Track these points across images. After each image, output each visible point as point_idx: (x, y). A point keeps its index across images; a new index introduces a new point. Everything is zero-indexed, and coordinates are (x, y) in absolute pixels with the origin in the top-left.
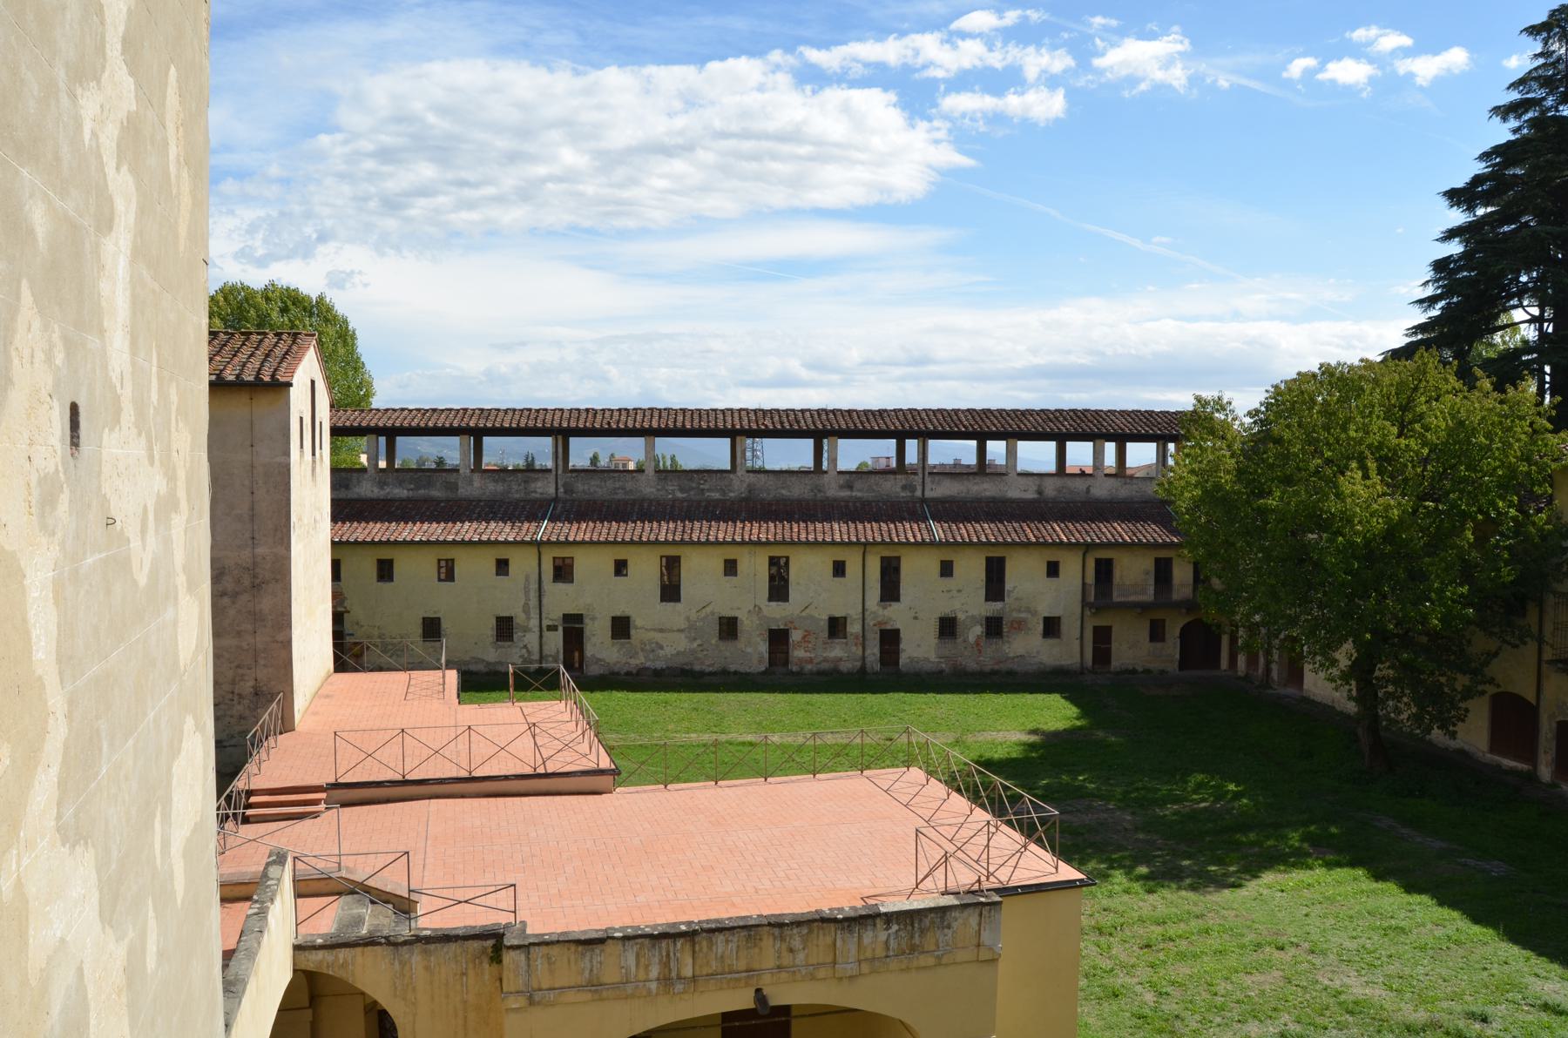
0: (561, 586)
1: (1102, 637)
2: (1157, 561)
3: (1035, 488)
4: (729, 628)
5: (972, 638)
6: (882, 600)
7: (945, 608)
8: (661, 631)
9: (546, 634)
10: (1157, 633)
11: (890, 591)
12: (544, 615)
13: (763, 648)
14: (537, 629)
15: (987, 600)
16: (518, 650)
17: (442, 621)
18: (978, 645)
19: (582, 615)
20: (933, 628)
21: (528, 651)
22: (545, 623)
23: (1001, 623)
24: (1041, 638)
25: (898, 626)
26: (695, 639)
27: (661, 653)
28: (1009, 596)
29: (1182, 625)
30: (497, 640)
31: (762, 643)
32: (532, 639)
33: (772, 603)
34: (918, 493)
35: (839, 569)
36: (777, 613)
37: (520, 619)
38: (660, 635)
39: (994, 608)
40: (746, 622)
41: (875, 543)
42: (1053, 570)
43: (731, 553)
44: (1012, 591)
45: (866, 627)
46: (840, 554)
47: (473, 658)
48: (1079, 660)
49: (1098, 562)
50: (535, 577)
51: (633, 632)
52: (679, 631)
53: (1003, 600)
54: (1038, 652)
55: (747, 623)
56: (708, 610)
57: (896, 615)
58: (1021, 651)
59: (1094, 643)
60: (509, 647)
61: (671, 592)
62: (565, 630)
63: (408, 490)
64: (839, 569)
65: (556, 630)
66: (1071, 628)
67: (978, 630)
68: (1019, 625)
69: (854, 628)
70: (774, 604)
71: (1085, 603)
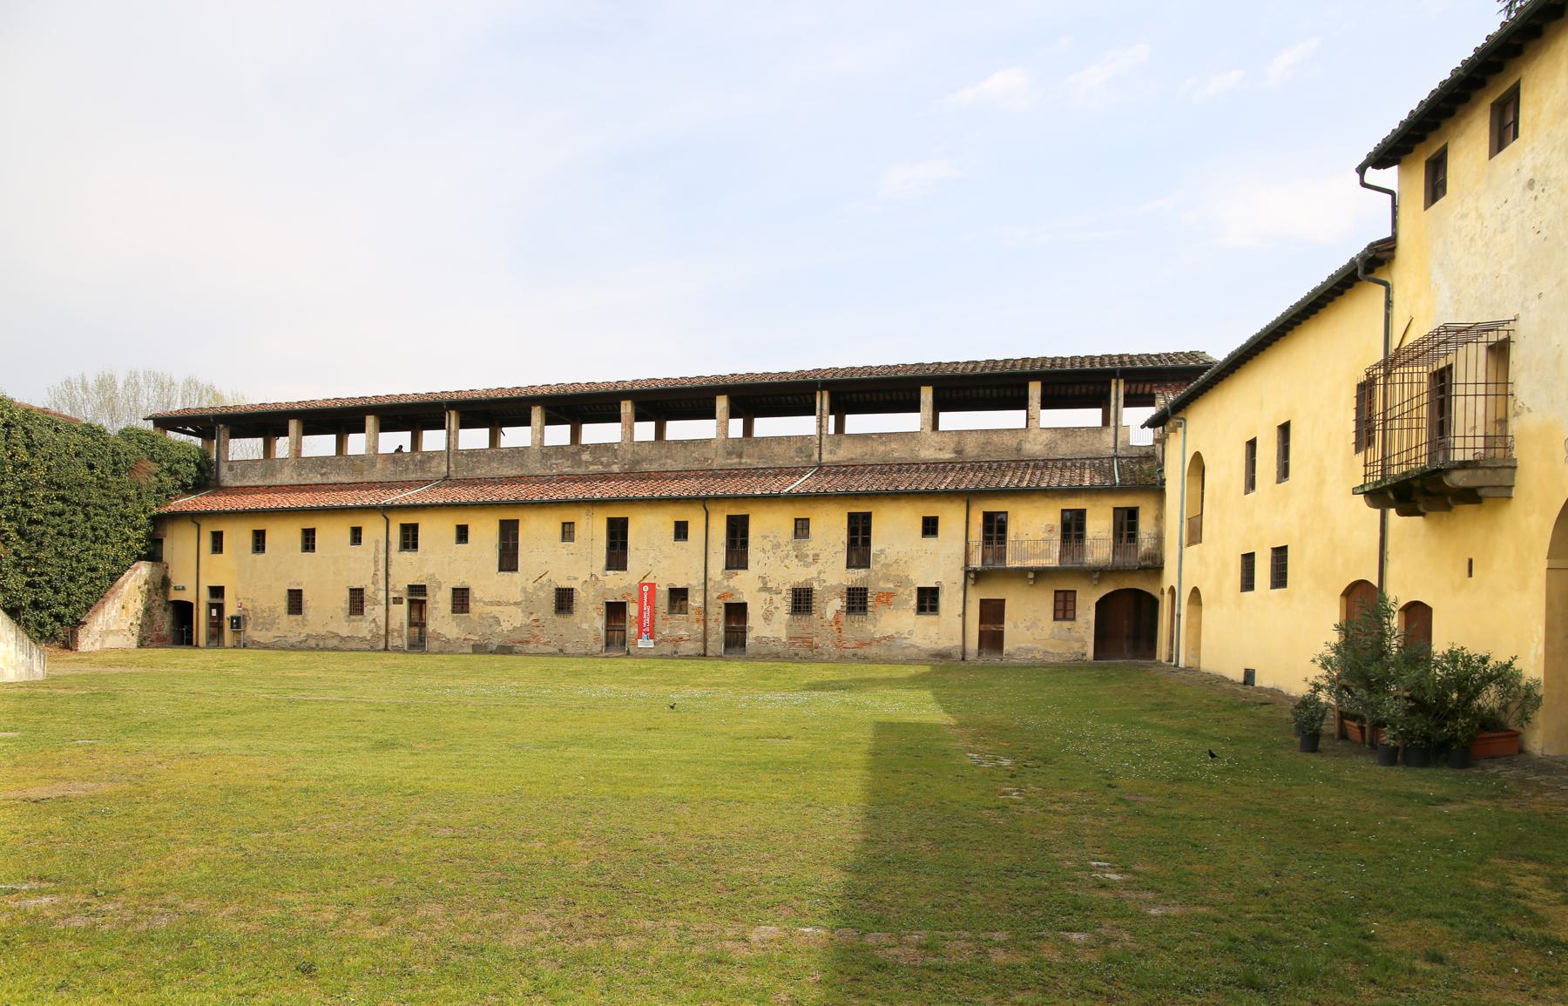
0: (407, 555)
1: (992, 612)
3: (952, 446)
4: (564, 600)
5: (830, 615)
6: (727, 568)
7: (799, 575)
8: (499, 604)
9: (393, 607)
10: (1064, 608)
12: (390, 587)
13: (600, 623)
14: (384, 602)
15: (848, 566)
16: (365, 624)
17: (304, 593)
18: (837, 623)
19: (425, 586)
20: (783, 605)
21: (377, 625)
22: (392, 595)
23: (866, 594)
25: (745, 599)
26: (532, 613)
27: (499, 630)
29: (1101, 596)
30: (351, 614)
31: (598, 618)
32: (380, 611)
33: (609, 572)
35: (681, 531)
36: (617, 584)
37: (368, 593)
38: (498, 608)
39: (856, 577)
40: (583, 594)
42: (930, 527)
45: (708, 598)
46: (682, 513)
47: (330, 632)
48: (959, 642)
51: (471, 605)
52: (516, 604)
54: (910, 633)
55: (581, 597)
56: (544, 579)
57: (744, 586)
58: (890, 631)
59: (981, 622)
60: (360, 620)
61: (508, 559)
62: (411, 602)
63: (322, 475)
64: (681, 531)
65: (402, 603)
66: (950, 602)
67: (837, 604)
68: (887, 598)
69: (695, 601)
70: (610, 573)
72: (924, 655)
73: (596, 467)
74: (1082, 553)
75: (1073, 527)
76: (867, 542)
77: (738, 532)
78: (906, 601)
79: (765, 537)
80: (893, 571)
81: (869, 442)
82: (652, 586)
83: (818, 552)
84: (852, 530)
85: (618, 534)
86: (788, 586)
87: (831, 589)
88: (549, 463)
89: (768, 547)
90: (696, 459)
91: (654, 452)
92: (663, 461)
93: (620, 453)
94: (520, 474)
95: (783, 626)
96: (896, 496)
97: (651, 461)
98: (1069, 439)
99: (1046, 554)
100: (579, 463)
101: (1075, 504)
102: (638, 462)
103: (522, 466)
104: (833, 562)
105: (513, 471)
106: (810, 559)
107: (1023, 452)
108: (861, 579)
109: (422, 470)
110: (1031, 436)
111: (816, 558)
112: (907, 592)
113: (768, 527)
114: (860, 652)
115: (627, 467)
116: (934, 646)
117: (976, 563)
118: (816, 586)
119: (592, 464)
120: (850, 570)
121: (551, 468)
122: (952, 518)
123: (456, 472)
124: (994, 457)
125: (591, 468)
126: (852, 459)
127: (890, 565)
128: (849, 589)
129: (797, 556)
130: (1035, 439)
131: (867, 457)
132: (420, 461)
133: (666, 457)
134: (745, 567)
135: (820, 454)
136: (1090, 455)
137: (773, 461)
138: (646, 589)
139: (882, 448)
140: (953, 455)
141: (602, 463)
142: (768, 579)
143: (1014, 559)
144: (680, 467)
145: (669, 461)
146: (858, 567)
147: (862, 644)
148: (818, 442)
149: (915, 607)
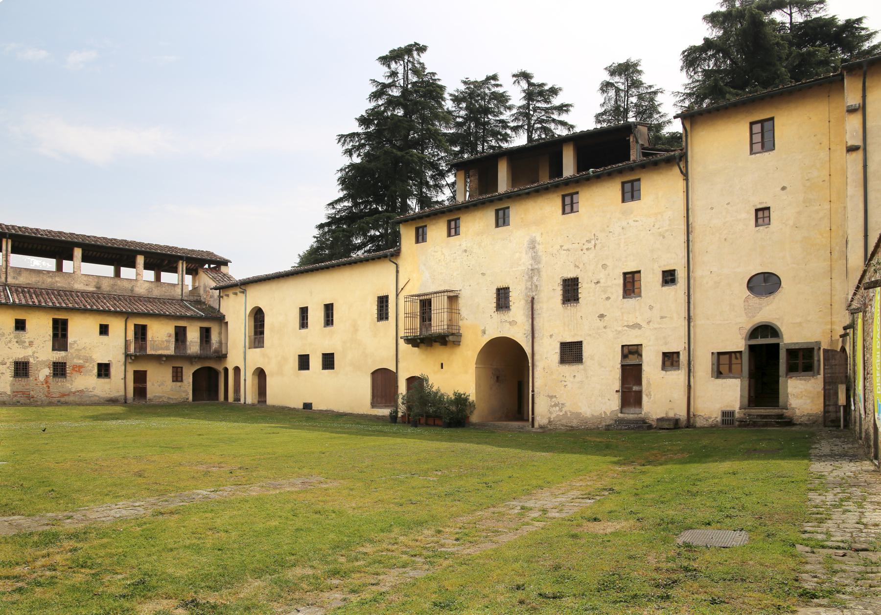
7: (20, 354)
15: (53, 350)
18: (46, 382)
23: (65, 366)
24: (95, 378)
28: (71, 348)
39: (59, 356)
49: (136, 326)
53: (67, 351)
58: (81, 387)
66: (117, 371)
67: (47, 371)
68: (79, 369)
71: (127, 356)
72: (102, 401)
74: (185, 348)
76: (65, 336)
78: (91, 371)
80: (83, 353)
83: (32, 340)
86: (11, 360)
87: (43, 362)
95: (8, 385)
96: (84, 311)
99: (167, 348)
101: (181, 323)
104: (43, 347)
111: (31, 344)
112: (91, 365)
114: (62, 399)
116: (109, 396)
117: (132, 350)
118: (31, 360)
120: (55, 352)
122: (117, 326)
127: (80, 350)
128: (54, 363)
129: (17, 342)
143: (151, 349)
147: (63, 395)
149: (96, 374)
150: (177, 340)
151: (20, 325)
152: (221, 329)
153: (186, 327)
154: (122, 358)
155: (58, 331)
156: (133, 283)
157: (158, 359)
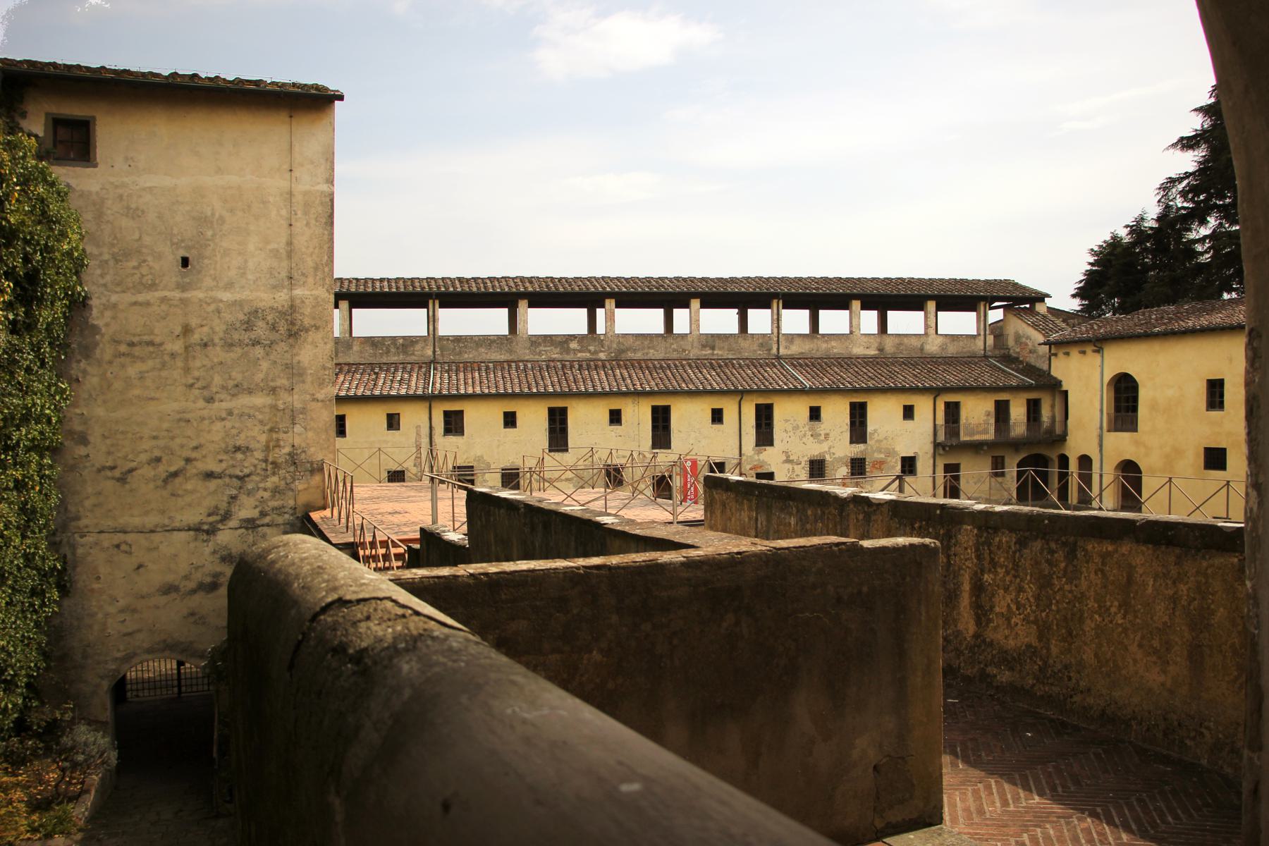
0: (452, 439)
2: (997, 403)
3: (876, 345)
6: (757, 445)
7: (814, 449)
11: (765, 435)
15: (851, 442)
25: (772, 469)
28: (871, 439)
29: (1019, 459)
34: (774, 351)
35: (717, 416)
39: (857, 450)
41: (751, 392)
42: (908, 412)
43: (615, 404)
44: (873, 434)
46: (717, 403)
49: (947, 405)
50: (425, 431)
53: (866, 442)
64: (717, 416)
71: (936, 445)
73: (584, 354)
74: (1008, 430)
75: (1002, 410)
77: (764, 418)
79: (787, 421)
80: (884, 445)
81: (815, 340)
82: (694, 463)
83: (828, 432)
84: (852, 415)
85: (661, 419)
86: (806, 459)
87: (840, 460)
88: (538, 350)
89: (789, 428)
90: (674, 350)
91: (638, 343)
92: (646, 351)
93: (606, 343)
94: (510, 358)
97: (635, 351)
98: (955, 343)
99: (985, 432)
100: (568, 351)
101: (1003, 396)
102: (623, 351)
103: (511, 351)
104: (840, 440)
105: (502, 357)
106: (822, 437)
107: (925, 351)
108: (861, 452)
109: (405, 353)
110: (930, 339)
111: (827, 436)
112: (894, 460)
113: (789, 413)
115: (613, 355)
117: (941, 437)
118: (828, 458)
119: (580, 351)
120: (853, 445)
121: (540, 354)
122: (923, 406)
123: (442, 355)
124: (905, 354)
125: (579, 355)
126: (802, 353)
127: (881, 441)
128: (852, 459)
129: (812, 436)
130: (932, 342)
131: (814, 352)
132: (403, 345)
133: (649, 348)
134: (771, 443)
135: (778, 349)
136: (969, 355)
137: (740, 353)
138: (689, 464)
139: (824, 346)
140: (877, 352)
141: (590, 351)
142: (790, 453)
143: (966, 434)
144: (661, 356)
145: (652, 351)
146: (858, 442)
148: (776, 339)
150: (997, 420)
151: (815, 414)
152: (1054, 400)
153: (1007, 402)
154: (929, 448)
155: (855, 417)
156: (923, 339)
157: (976, 448)
